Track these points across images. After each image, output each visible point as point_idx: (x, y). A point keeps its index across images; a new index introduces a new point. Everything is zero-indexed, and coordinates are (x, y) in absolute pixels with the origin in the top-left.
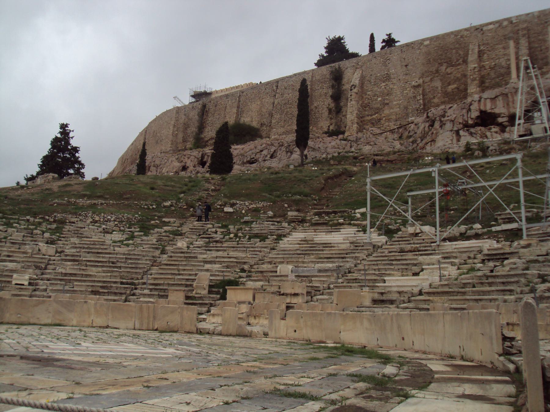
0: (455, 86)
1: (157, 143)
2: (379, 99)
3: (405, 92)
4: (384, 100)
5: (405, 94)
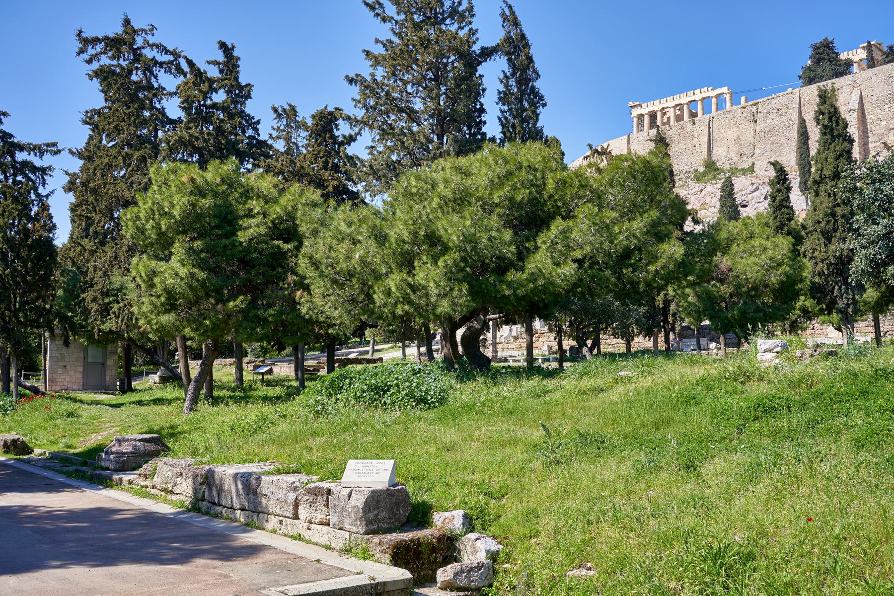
2: (883, 123)
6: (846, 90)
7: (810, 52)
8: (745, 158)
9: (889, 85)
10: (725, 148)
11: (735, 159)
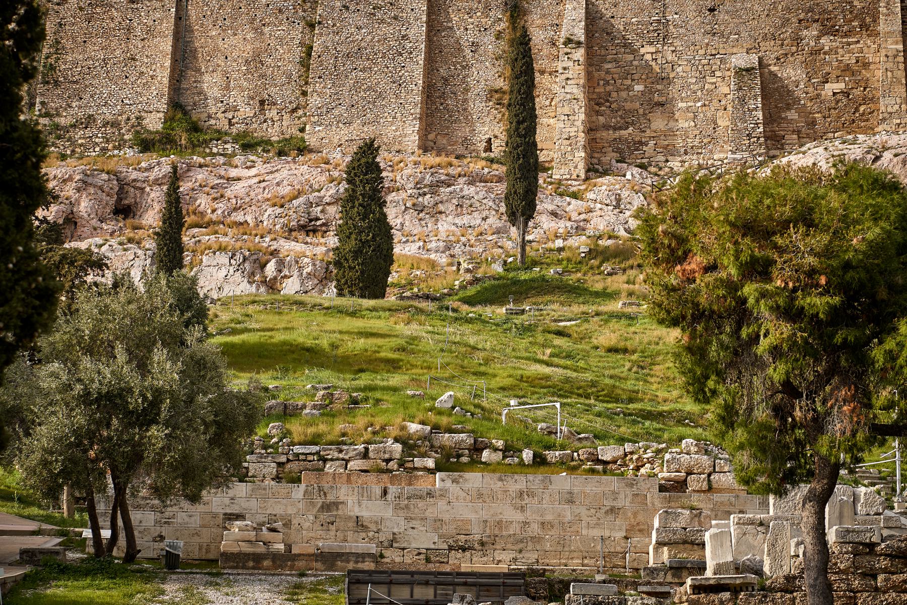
0: (841, 86)
2: (639, 88)
4: (651, 92)
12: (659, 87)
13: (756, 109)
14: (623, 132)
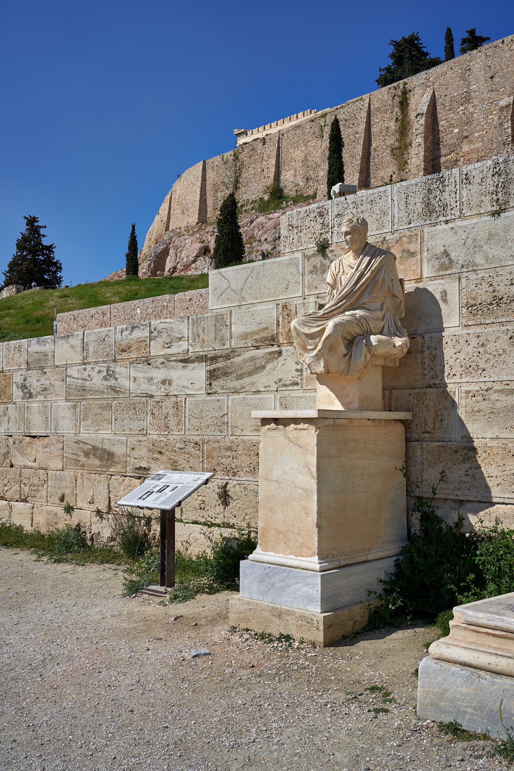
1: (183, 213)
2: (456, 131)
3: (490, 117)
4: (462, 132)
5: (489, 121)
6: (418, 91)
7: (391, 49)
8: (311, 183)
9: (465, 80)
10: (292, 172)
11: (302, 184)
12: (466, 128)
13: (508, 128)
14: (449, 157)
